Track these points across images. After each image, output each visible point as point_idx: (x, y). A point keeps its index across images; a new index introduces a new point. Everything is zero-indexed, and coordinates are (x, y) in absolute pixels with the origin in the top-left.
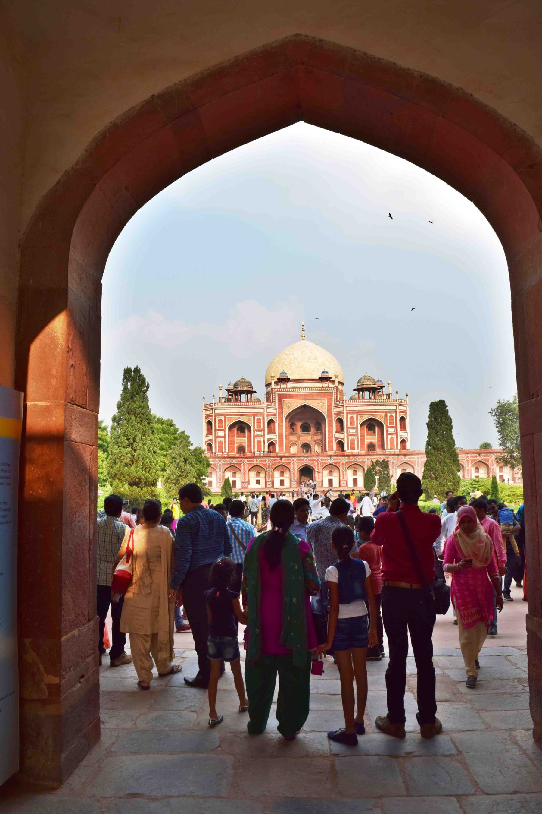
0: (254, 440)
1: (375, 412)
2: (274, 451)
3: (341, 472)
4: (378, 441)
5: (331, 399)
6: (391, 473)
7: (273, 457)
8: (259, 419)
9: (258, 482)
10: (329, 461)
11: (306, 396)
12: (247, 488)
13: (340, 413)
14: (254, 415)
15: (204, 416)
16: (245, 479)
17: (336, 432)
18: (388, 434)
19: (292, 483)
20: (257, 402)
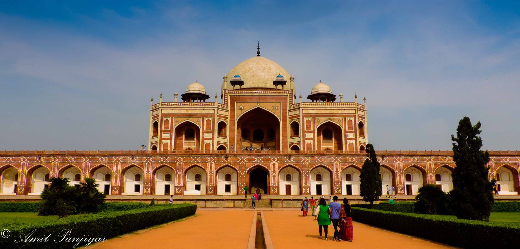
0: (203, 142)
1: (333, 116)
3: (303, 176)
4: (335, 147)
8: (208, 121)
9: (198, 187)
10: (287, 161)
11: (260, 98)
12: (182, 194)
13: (295, 117)
14: (203, 116)
15: (151, 117)
16: (179, 183)
17: (291, 137)
18: (346, 139)
19: (240, 189)
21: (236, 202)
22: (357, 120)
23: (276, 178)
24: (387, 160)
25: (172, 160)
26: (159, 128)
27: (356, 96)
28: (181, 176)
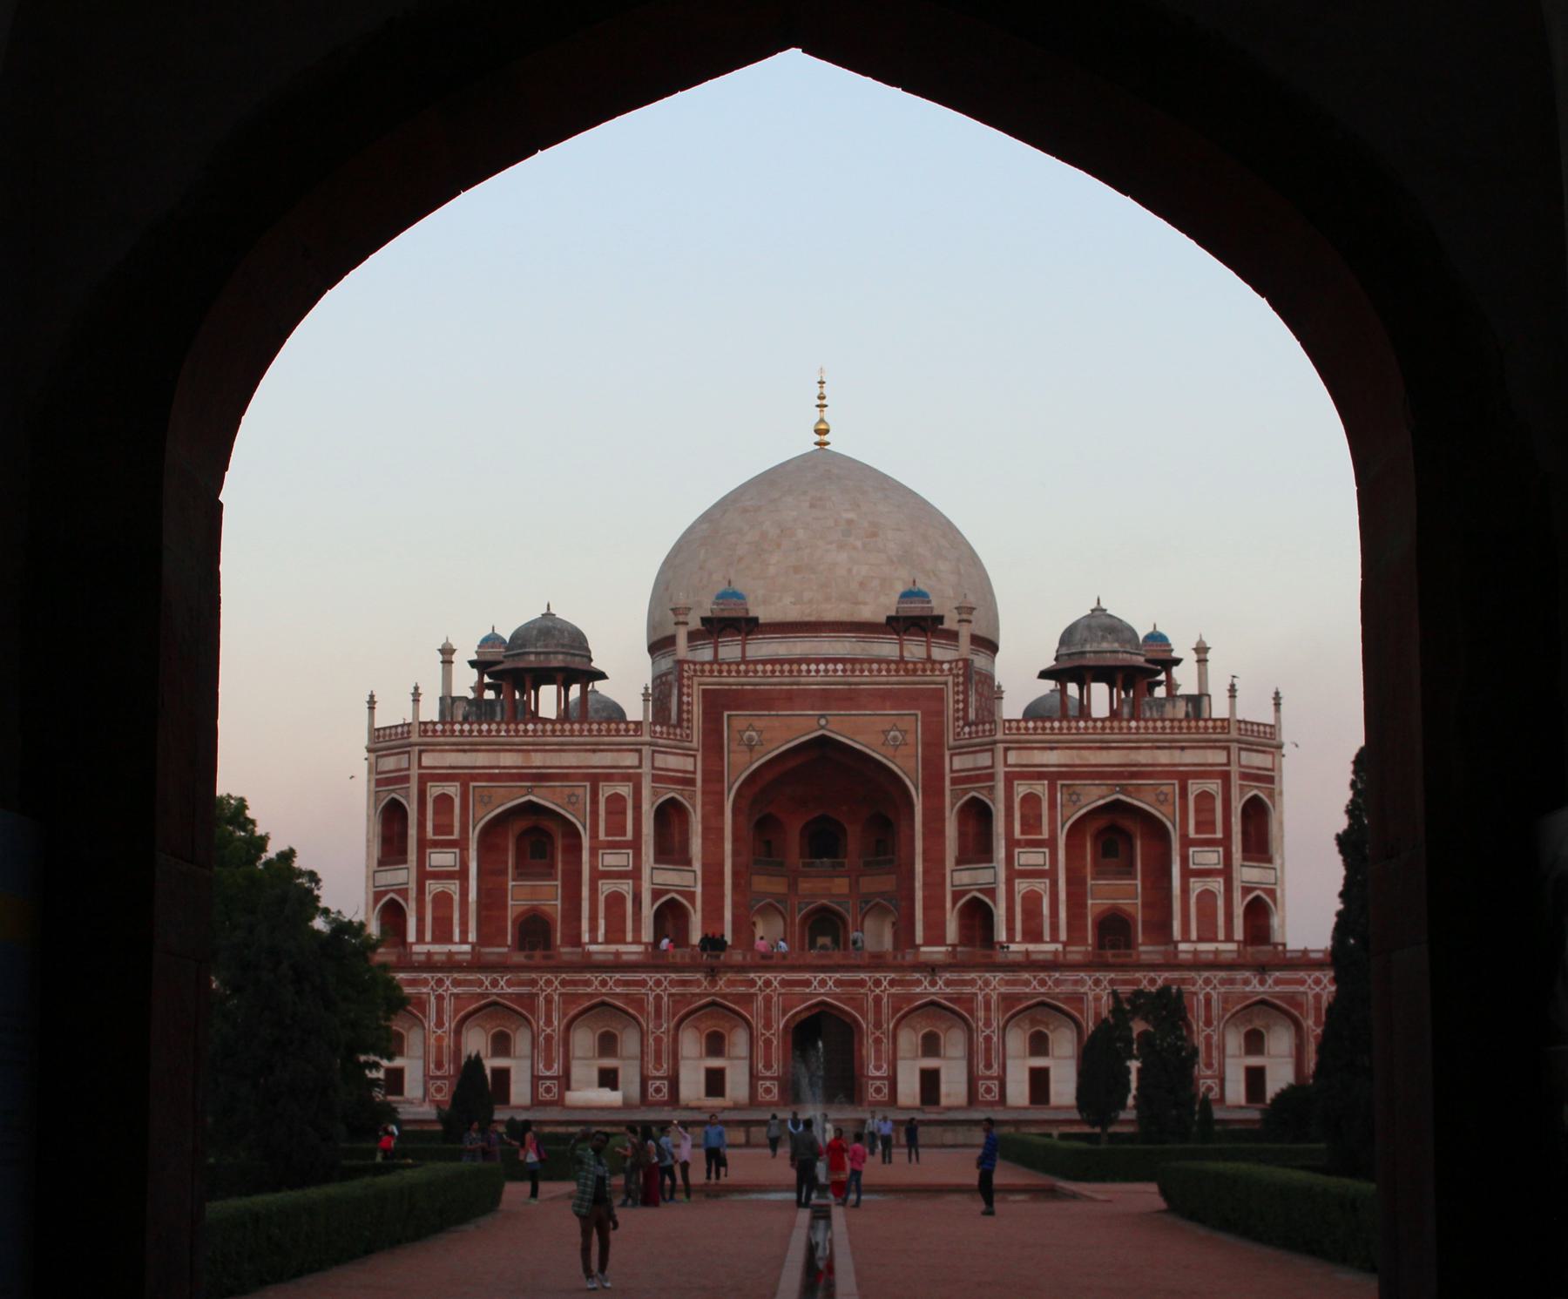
0: (594, 891)
1: (1133, 775)
2: (681, 939)
5: (940, 713)
6: (1199, 1041)
7: (676, 968)
8: (616, 799)
9: (608, 1079)
12: (559, 1102)
13: (978, 779)
14: (595, 779)
17: (959, 862)
18: (1187, 873)
20: (609, 721)
21: (753, 1129)
22: (1235, 792)
23: (886, 1045)
24: (1277, 982)
25: (521, 984)
26: (413, 832)
27: (1232, 690)
28: (555, 1042)
